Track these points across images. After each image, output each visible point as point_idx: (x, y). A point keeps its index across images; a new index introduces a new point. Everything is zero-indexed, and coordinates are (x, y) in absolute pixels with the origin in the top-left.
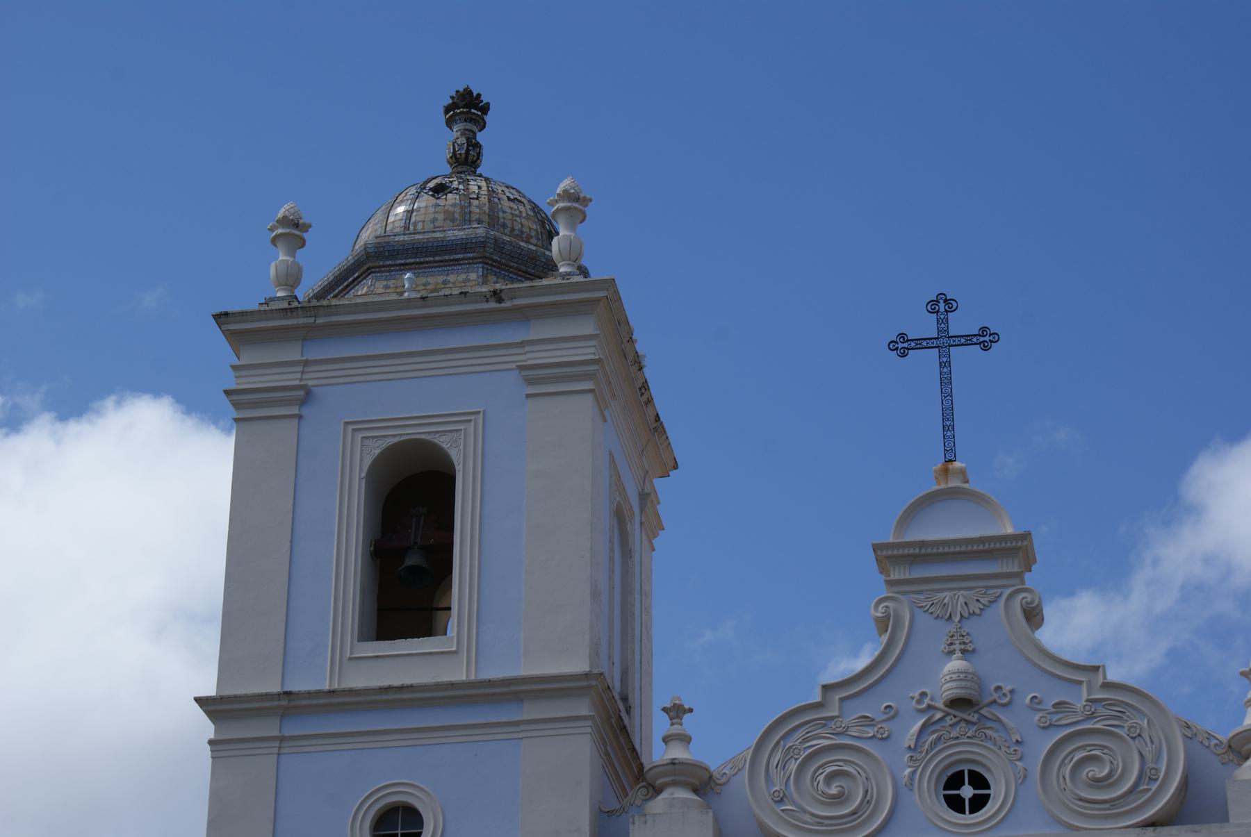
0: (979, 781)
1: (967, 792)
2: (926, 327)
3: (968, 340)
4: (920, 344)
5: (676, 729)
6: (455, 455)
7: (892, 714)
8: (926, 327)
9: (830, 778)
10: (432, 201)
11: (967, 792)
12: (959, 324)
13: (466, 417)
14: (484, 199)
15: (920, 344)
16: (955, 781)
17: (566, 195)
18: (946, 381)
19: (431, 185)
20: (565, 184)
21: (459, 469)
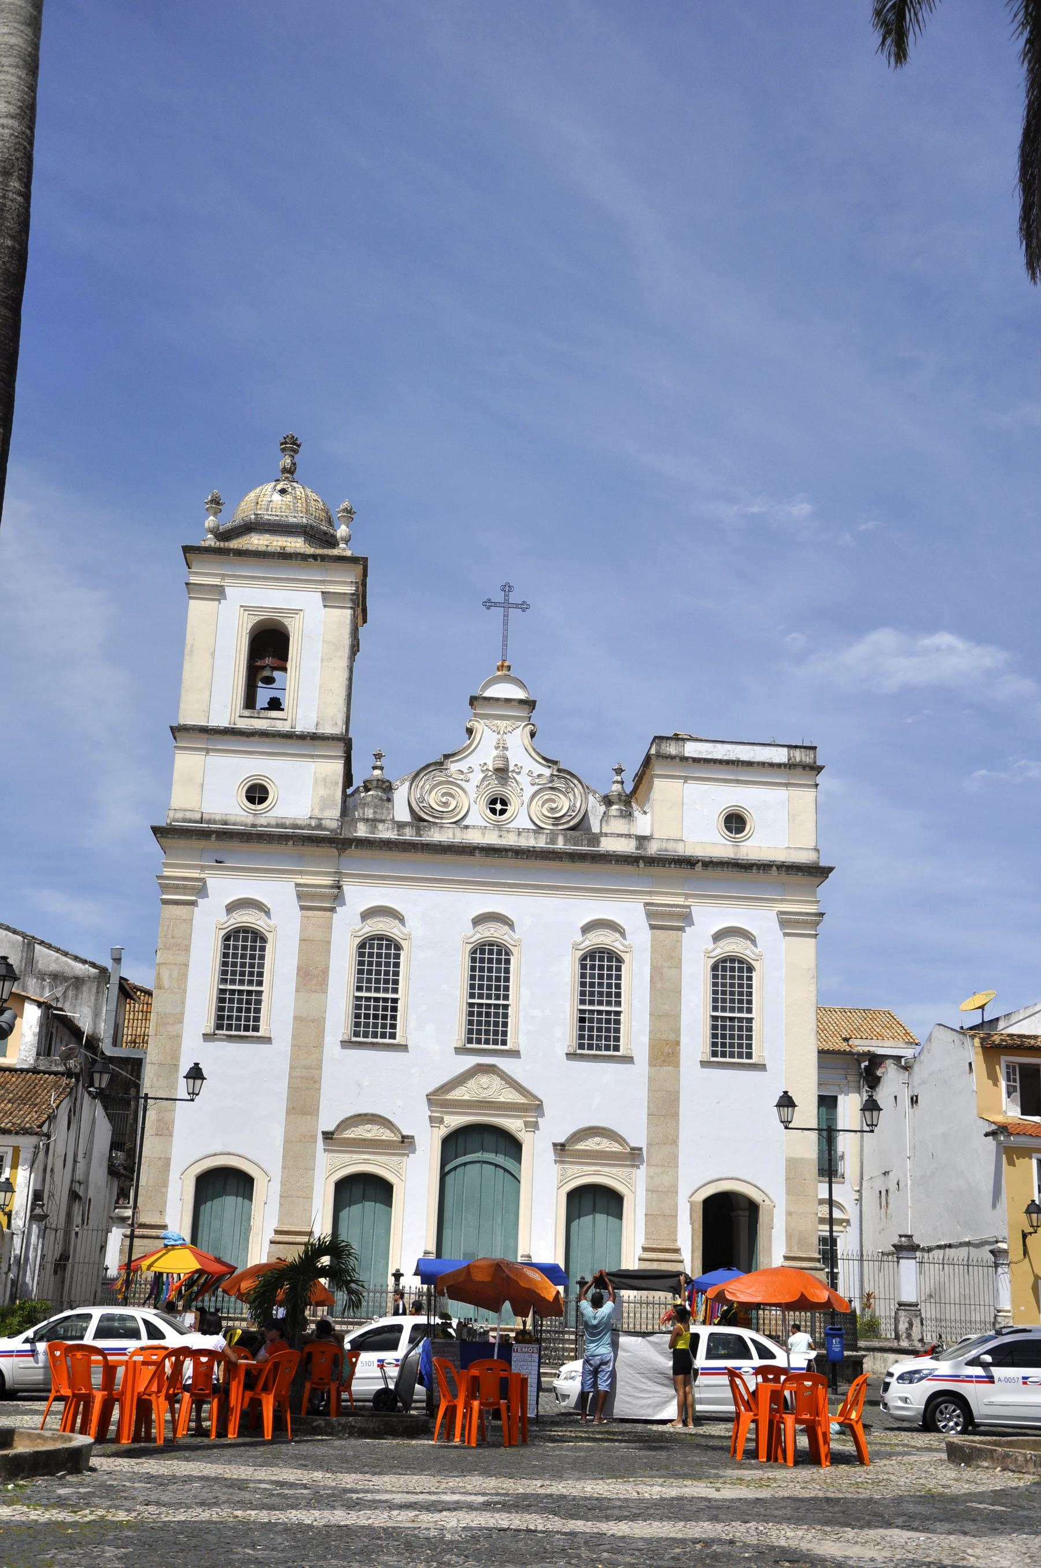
0: (504, 803)
1: (498, 807)
2: (499, 597)
3: (517, 606)
4: (496, 604)
5: (378, 764)
6: (291, 629)
7: (471, 770)
8: (499, 597)
9: (444, 795)
10: (280, 498)
11: (498, 807)
12: (514, 598)
13: (296, 612)
14: (303, 500)
15: (496, 604)
16: (494, 802)
17: (346, 510)
18: (506, 624)
20: (346, 504)
21: (291, 634)
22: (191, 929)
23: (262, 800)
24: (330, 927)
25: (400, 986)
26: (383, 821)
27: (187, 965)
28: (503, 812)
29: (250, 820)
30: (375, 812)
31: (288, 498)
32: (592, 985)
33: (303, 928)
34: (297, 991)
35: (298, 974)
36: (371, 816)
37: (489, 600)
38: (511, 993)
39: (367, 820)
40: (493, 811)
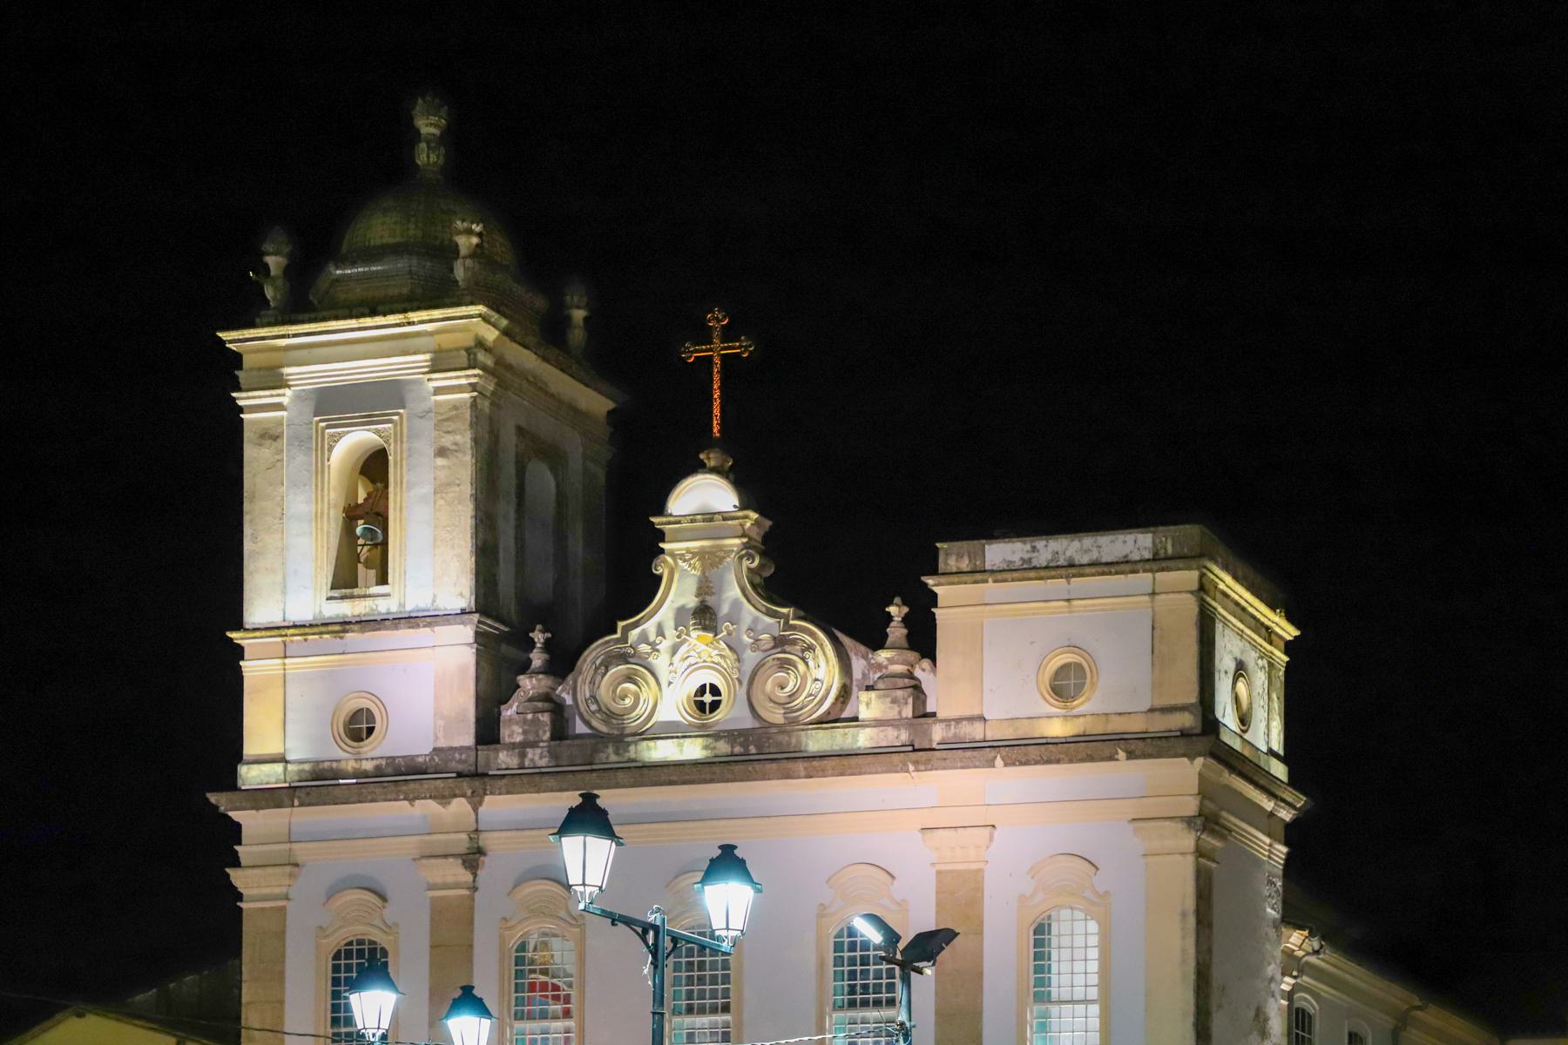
11: (708, 698)
16: (702, 690)
23: (370, 731)
24: (471, 922)
26: (534, 745)
27: (282, 1002)
28: (715, 706)
30: (524, 732)
36: (519, 739)
39: (513, 746)
40: (701, 706)
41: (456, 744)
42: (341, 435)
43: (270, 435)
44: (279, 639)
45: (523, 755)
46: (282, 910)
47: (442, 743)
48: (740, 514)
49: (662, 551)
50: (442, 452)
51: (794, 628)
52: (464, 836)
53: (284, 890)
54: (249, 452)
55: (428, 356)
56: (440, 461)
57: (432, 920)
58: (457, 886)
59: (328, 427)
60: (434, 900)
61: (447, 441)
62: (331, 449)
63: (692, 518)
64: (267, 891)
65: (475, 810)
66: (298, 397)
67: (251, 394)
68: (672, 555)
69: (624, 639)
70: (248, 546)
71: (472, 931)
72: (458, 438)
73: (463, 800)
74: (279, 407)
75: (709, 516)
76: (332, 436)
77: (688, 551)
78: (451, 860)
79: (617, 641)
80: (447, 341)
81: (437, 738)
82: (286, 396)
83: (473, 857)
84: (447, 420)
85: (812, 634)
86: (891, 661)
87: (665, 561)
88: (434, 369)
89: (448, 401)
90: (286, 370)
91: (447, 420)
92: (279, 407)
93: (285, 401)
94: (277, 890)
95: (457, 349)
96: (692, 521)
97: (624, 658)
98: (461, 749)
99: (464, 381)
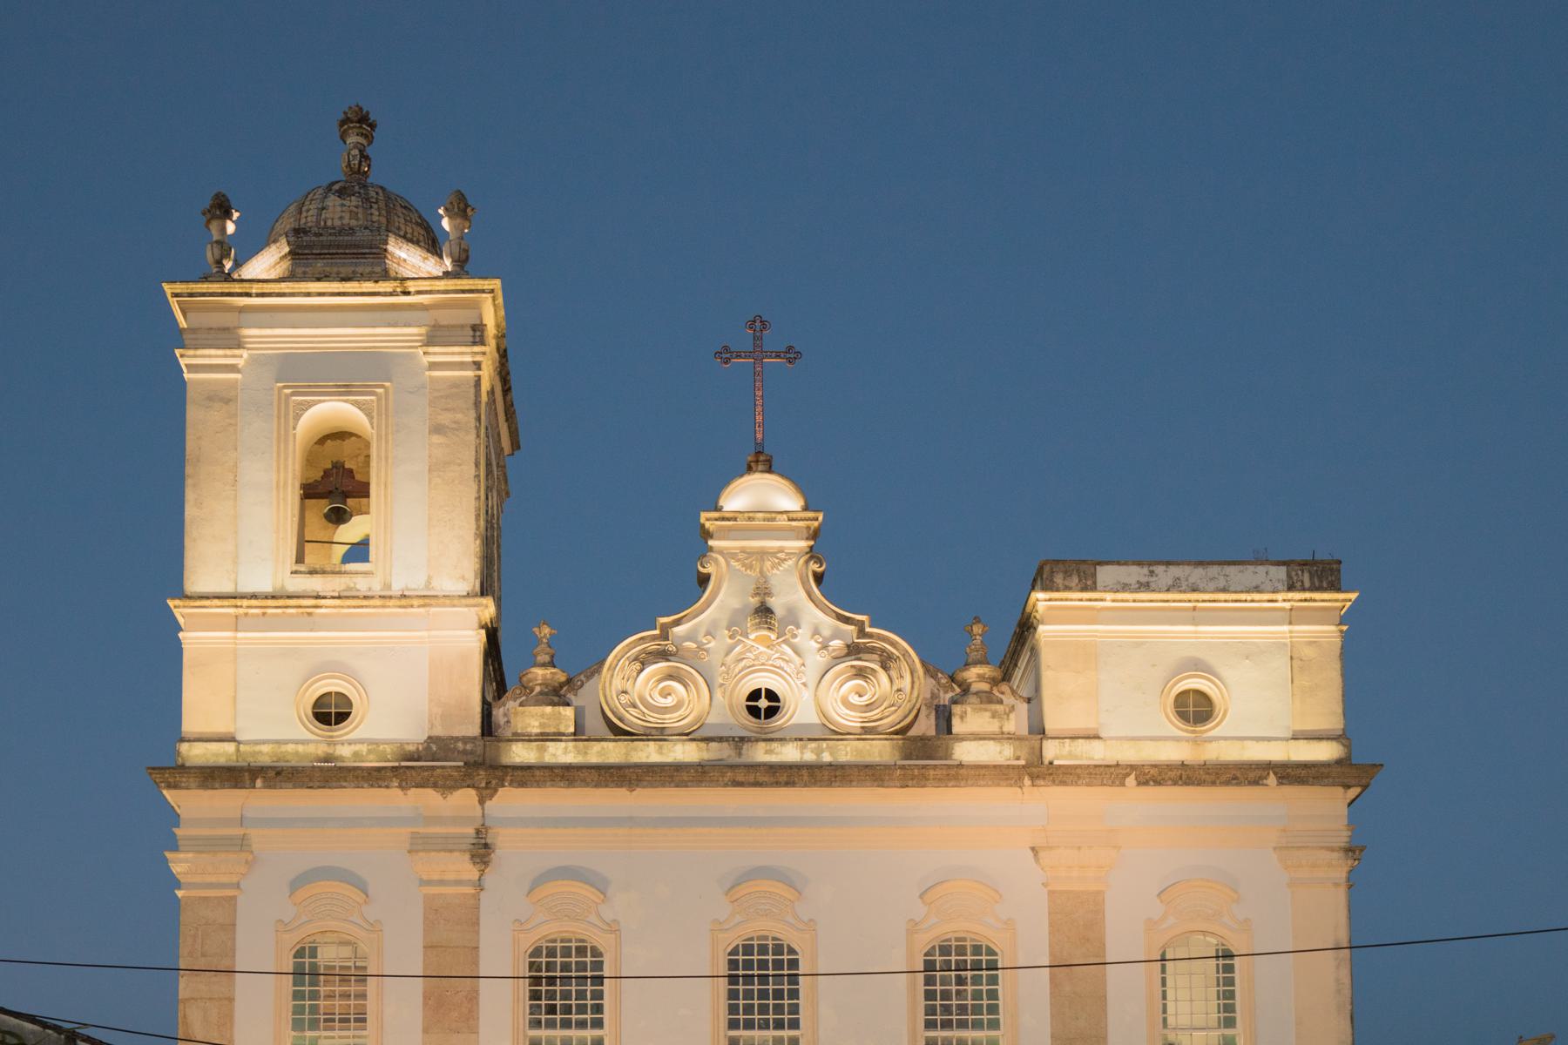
1: (763, 703)
8: (745, 340)
10: (339, 201)
11: (763, 703)
14: (382, 204)
19: (336, 187)
22: (234, 939)
24: (476, 923)
25: (607, 1016)
28: (772, 712)
29: (322, 749)
31: (354, 201)
32: (946, 995)
33: (429, 925)
34: (426, 1031)
35: (425, 1004)
37: (726, 349)
38: (803, 1016)
40: (754, 711)
41: (456, 734)
42: (310, 405)
43: (222, 398)
44: (232, 611)
45: (542, 750)
46: (234, 898)
47: (439, 731)
48: (810, 515)
49: (711, 549)
50: (437, 429)
51: (870, 636)
52: (471, 831)
53: (235, 880)
54: (193, 413)
55: (423, 330)
56: (436, 439)
57: (426, 918)
58: (458, 883)
59: (293, 394)
60: (428, 899)
61: (445, 419)
62: (298, 417)
63: (749, 515)
64: (213, 879)
65: (482, 802)
66: (255, 361)
67: (200, 352)
68: (721, 552)
69: (664, 636)
70: (190, 511)
71: (478, 933)
72: (459, 416)
73: (472, 792)
74: (232, 368)
75: (772, 514)
76: (301, 403)
77: (743, 550)
78: (456, 854)
79: (654, 638)
80: (446, 317)
81: (432, 726)
82: (241, 358)
83: (482, 851)
84: (447, 397)
85: (893, 644)
86: (981, 678)
87: (716, 561)
88: (430, 341)
89: (447, 378)
90: (246, 332)
91: (447, 397)
92: (232, 368)
93: (240, 362)
94: (225, 879)
95: (462, 326)
96: (750, 519)
97: (664, 655)
98: (465, 740)
99: (468, 359)
